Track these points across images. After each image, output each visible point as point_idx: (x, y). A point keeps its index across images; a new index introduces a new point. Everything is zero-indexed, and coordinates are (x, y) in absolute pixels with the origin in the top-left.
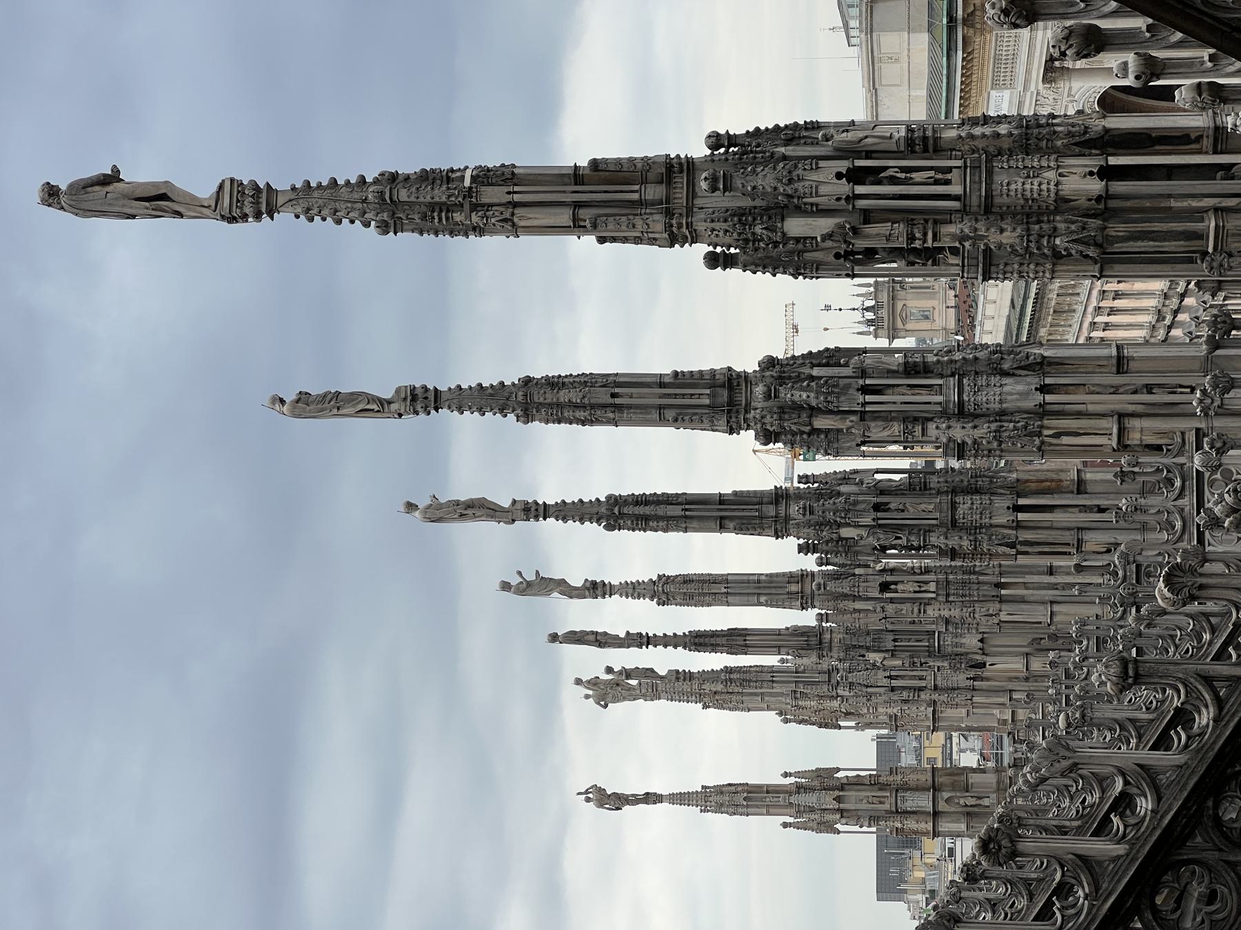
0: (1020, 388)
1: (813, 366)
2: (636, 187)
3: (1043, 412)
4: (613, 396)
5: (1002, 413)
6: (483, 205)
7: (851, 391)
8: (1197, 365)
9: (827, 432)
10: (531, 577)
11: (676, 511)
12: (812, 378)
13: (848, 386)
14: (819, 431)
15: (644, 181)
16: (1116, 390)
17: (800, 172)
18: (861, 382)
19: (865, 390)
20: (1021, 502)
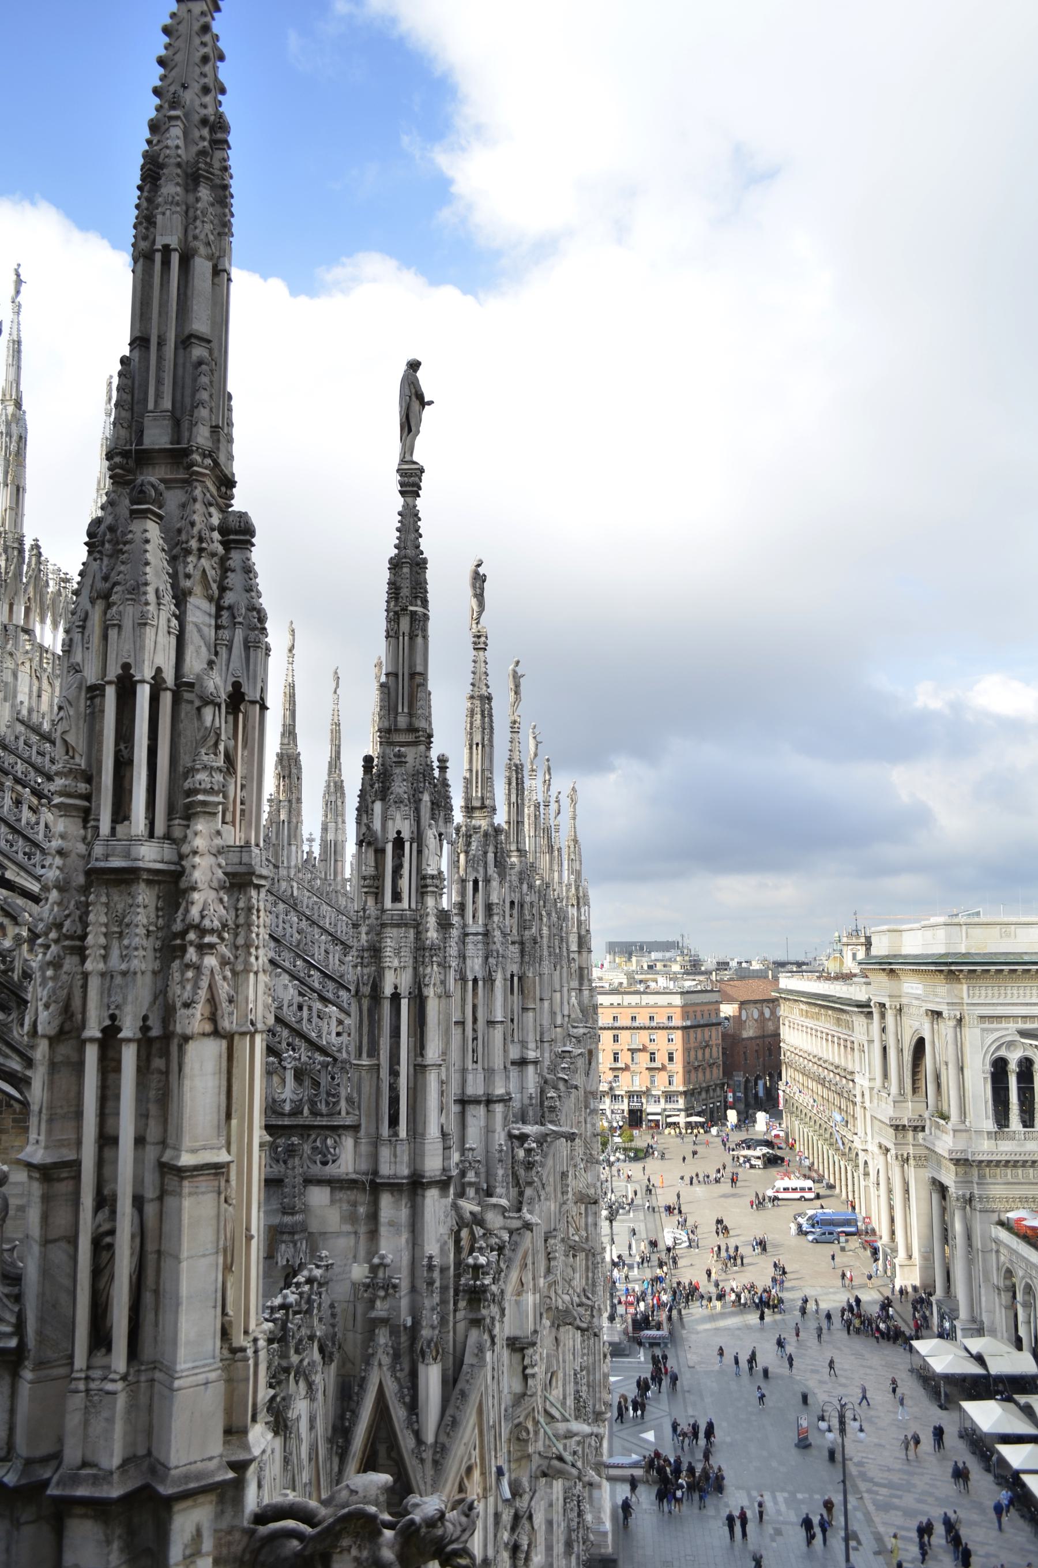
0: (477, 967)
1: (496, 854)
2: (406, 710)
3: (463, 979)
4: (477, 744)
5: (463, 957)
6: (398, 619)
7: (475, 874)
8: (491, 1065)
9: (458, 861)
10: (538, 739)
11: (513, 799)
12: (486, 853)
13: (478, 871)
14: (458, 857)
15: (411, 715)
16: (475, 1020)
17: (403, 808)
18: (480, 879)
19: (476, 882)
20: (516, 979)
